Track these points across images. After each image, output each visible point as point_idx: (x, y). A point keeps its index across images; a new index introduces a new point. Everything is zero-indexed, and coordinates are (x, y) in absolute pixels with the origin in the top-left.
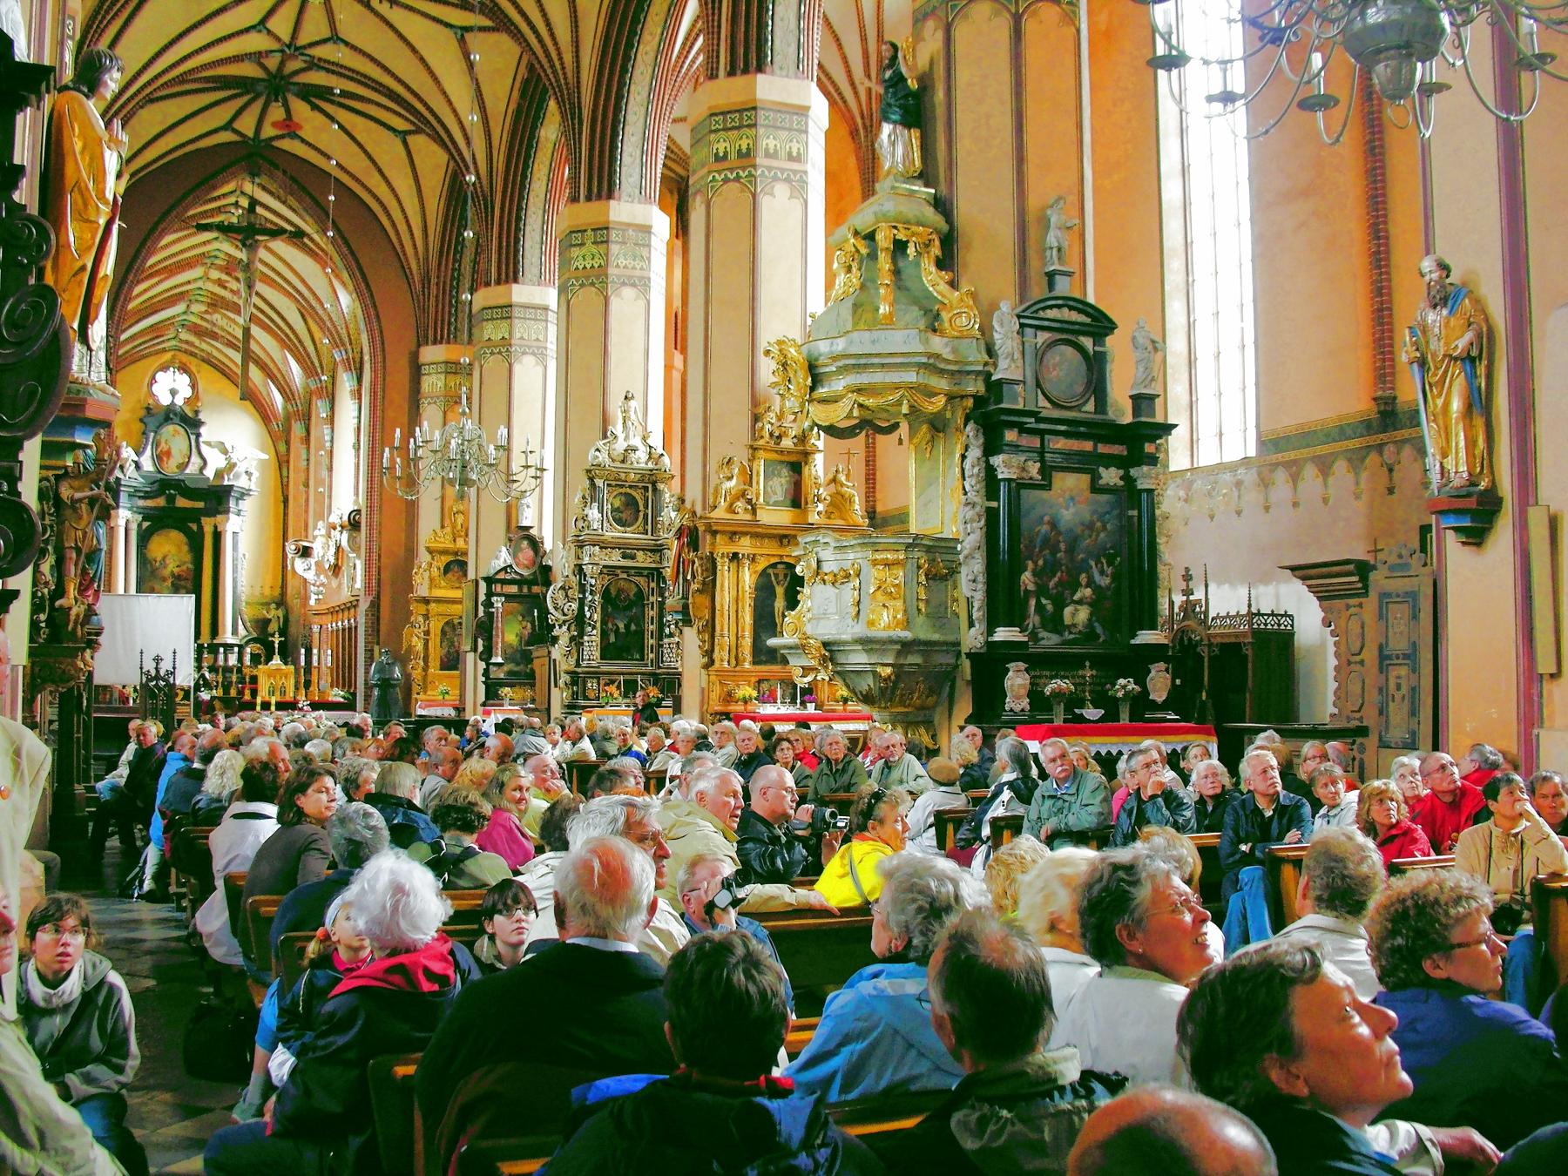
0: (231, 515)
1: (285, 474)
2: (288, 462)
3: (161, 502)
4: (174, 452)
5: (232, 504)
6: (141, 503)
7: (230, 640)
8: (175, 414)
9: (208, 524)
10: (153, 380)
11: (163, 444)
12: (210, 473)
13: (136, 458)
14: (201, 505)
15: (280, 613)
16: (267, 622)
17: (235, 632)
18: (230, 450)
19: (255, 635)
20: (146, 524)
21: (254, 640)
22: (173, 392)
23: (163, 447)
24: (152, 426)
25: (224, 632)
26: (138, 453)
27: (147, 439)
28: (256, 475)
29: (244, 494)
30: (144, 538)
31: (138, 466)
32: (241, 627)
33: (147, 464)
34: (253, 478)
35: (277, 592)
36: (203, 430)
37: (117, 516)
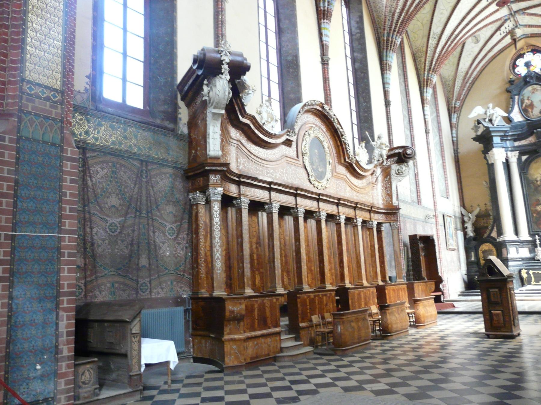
3: (531, 140)
4: (535, 104)
6: (517, 144)
8: (532, 78)
10: (514, 66)
11: (527, 102)
13: (506, 115)
20: (524, 158)
22: (528, 65)
23: (527, 102)
24: (515, 92)
26: (509, 110)
27: (513, 101)
30: (524, 168)
31: (509, 120)
33: (517, 117)
37: (493, 154)
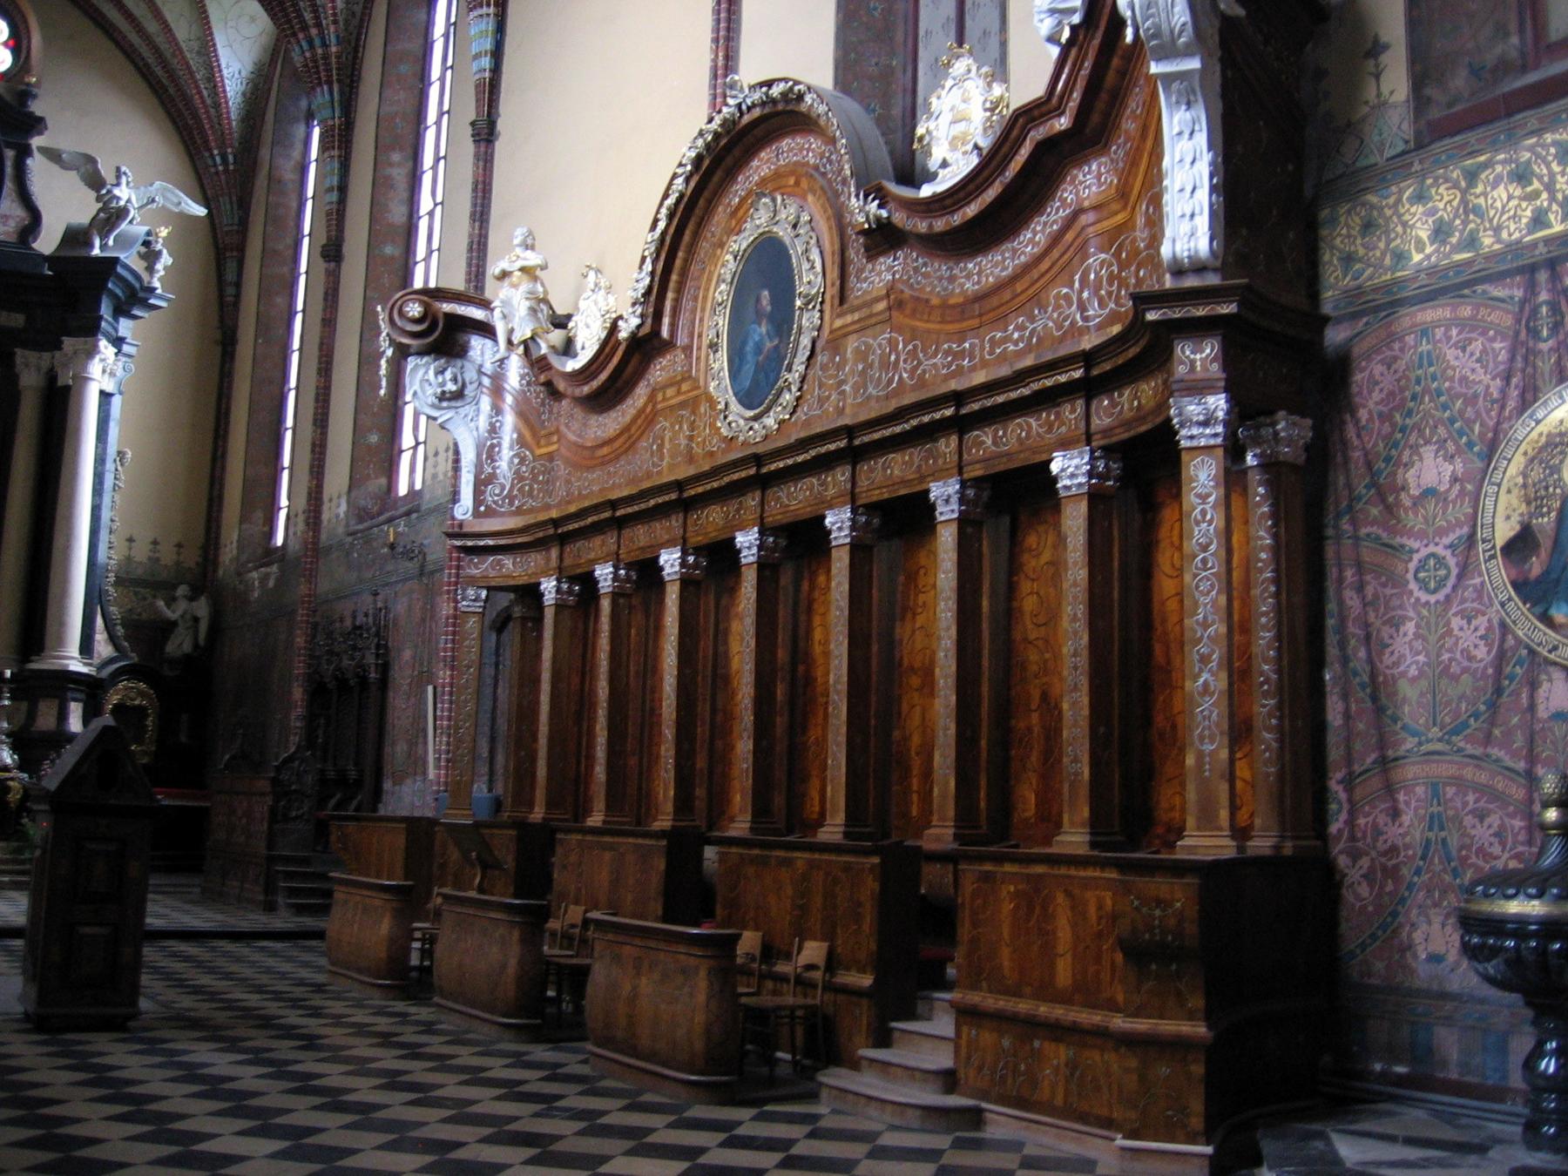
0: (103, 344)
1: (230, 276)
2: (241, 249)
5: (105, 310)
7: (77, 666)
9: (29, 371)
12: (47, 243)
14: (17, 320)
15: (202, 608)
16: (168, 627)
17: (86, 648)
18: (110, 177)
19: (134, 658)
21: (131, 672)
25: (61, 642)
28: (166, 260)
29: (134, 299)
32: (100, 636)
34: (159, 266)
35: (191, 558)
36: (36, 142)
